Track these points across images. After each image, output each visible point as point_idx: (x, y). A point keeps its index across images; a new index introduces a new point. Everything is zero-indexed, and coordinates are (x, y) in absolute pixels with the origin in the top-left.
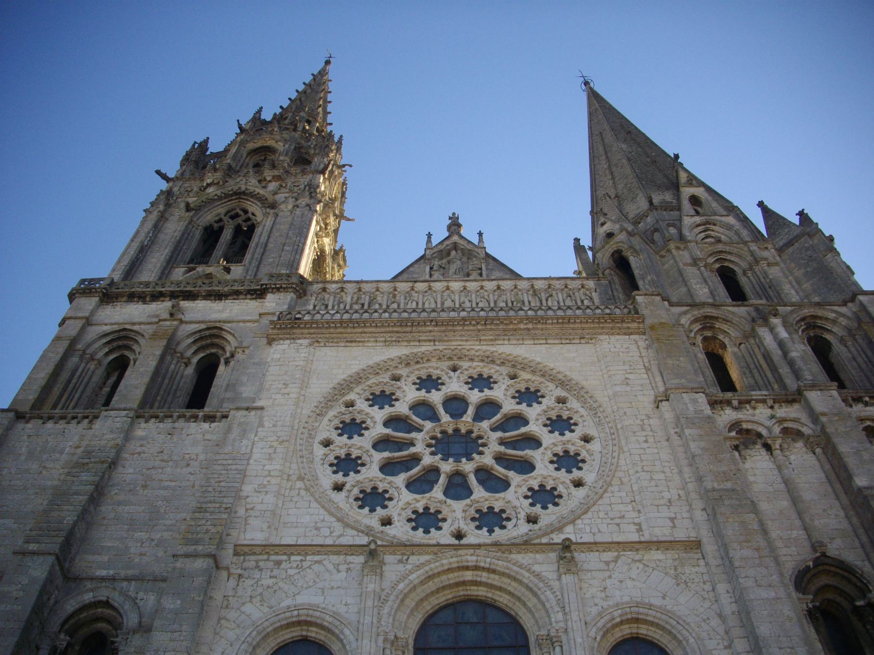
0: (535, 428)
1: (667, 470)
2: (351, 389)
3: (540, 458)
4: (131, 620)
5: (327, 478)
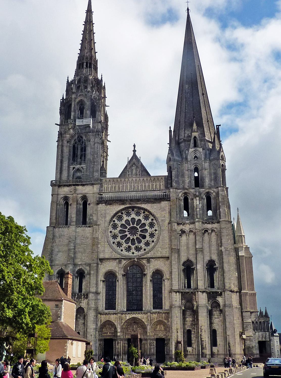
0: (147, 227)
1: (167, 240)
2: (113, 218)
3: (147, 235)
4: (86, 272)
5: (112, 240)
